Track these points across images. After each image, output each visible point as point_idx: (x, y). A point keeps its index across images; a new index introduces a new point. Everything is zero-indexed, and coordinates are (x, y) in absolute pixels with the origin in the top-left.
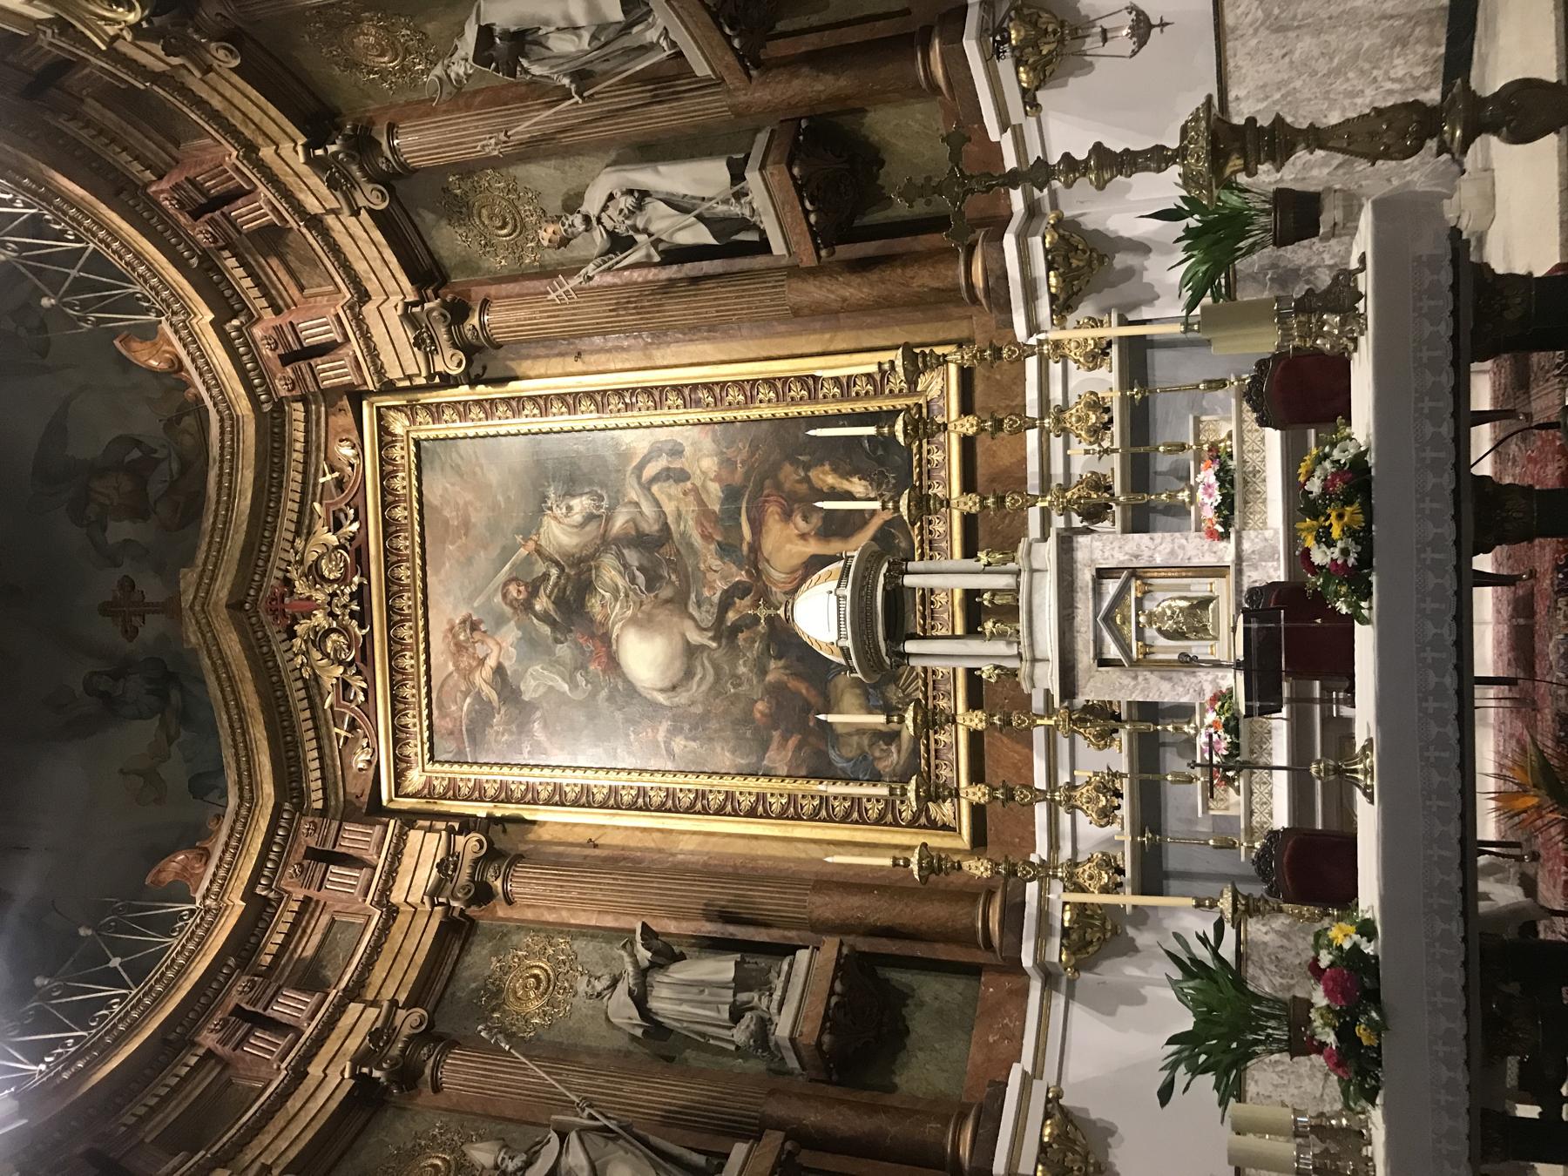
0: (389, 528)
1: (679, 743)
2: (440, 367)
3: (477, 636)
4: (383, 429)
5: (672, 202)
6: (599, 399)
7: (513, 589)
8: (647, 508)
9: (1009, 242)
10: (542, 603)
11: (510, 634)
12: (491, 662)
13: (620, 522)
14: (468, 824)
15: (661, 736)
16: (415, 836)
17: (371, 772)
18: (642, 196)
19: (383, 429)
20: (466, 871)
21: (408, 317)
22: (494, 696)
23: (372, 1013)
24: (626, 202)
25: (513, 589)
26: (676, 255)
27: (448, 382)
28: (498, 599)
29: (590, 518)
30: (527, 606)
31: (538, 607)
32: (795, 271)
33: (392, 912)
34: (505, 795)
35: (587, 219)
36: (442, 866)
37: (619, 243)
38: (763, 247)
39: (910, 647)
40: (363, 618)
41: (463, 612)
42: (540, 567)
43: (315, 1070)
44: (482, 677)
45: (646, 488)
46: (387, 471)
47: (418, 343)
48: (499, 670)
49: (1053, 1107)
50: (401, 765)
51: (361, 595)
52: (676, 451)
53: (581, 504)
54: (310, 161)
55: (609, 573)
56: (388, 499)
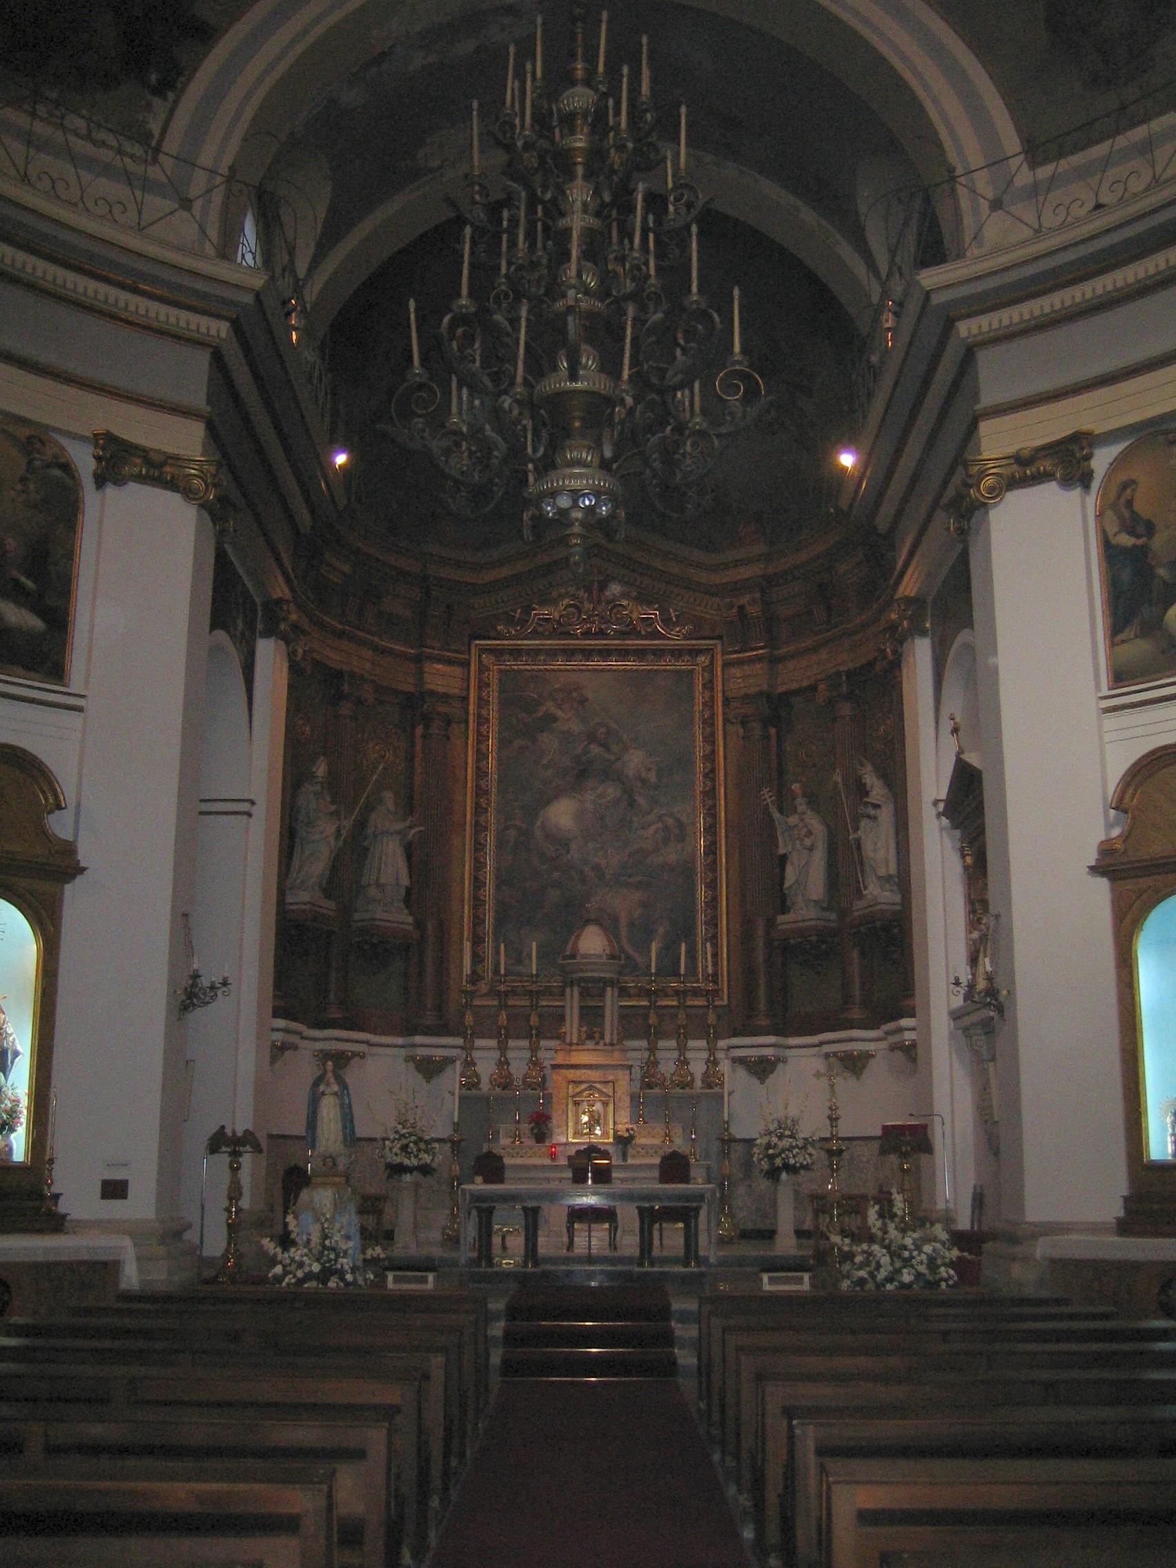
0: (641, 653)
1: (512, 833)
2: (733, 704)
3: (575, 704)
4: (699, 652)
5: (807, 864)
6: (710, 793)
7: (603, 730)
8: (650, 818)
9: (771, 1039)
10: (595, 749)
11: (577, 727)
12: (559, 713)
13: (641, 800)
14: (465, 699)
15: (518, 823)
16: (458, 671)
17: (492, 634)
18: (811, 849)
19: (699, 652)
20: (442, 709)
21: (761, 694)
22: (540, 714)
23: (368, 666)
24: (808, 842)
25: (603, 730)
26: (783, 859)
27: (726, 701)
28: (597, 720)
29: (644, 781)
30: (592, 738)
31: (592, 746)
32: (771, 923)
33: (419, 659)
34: (482, 720)
35: (804, 813)
36: (446, 696)
37: (791, 828)
38: (784, 909)
39: (576, 990)
40: (587, 634)
41: (590, 695)
42: (615, 748)
43: (345, 645)
44: (550, 706)
45: (660, 818)
46: (677, 653)
47: (746, 696)
48: (554, 719)
49: (355, 1054)
50: (497, 652)
51: (601, 634)
52: (682, 838)
53: (652, 777)
54: (838, 674)
55: (612, 791)
56: (659, 653)
